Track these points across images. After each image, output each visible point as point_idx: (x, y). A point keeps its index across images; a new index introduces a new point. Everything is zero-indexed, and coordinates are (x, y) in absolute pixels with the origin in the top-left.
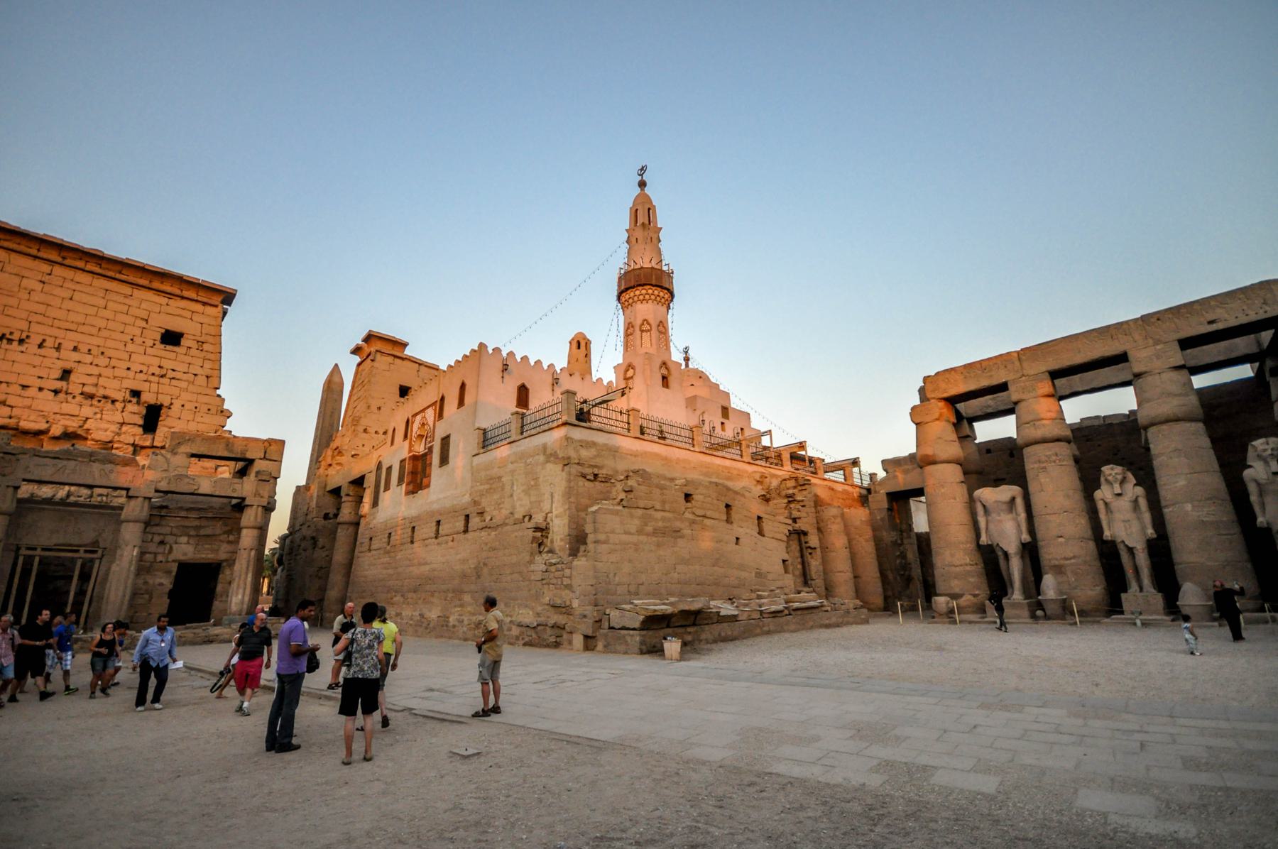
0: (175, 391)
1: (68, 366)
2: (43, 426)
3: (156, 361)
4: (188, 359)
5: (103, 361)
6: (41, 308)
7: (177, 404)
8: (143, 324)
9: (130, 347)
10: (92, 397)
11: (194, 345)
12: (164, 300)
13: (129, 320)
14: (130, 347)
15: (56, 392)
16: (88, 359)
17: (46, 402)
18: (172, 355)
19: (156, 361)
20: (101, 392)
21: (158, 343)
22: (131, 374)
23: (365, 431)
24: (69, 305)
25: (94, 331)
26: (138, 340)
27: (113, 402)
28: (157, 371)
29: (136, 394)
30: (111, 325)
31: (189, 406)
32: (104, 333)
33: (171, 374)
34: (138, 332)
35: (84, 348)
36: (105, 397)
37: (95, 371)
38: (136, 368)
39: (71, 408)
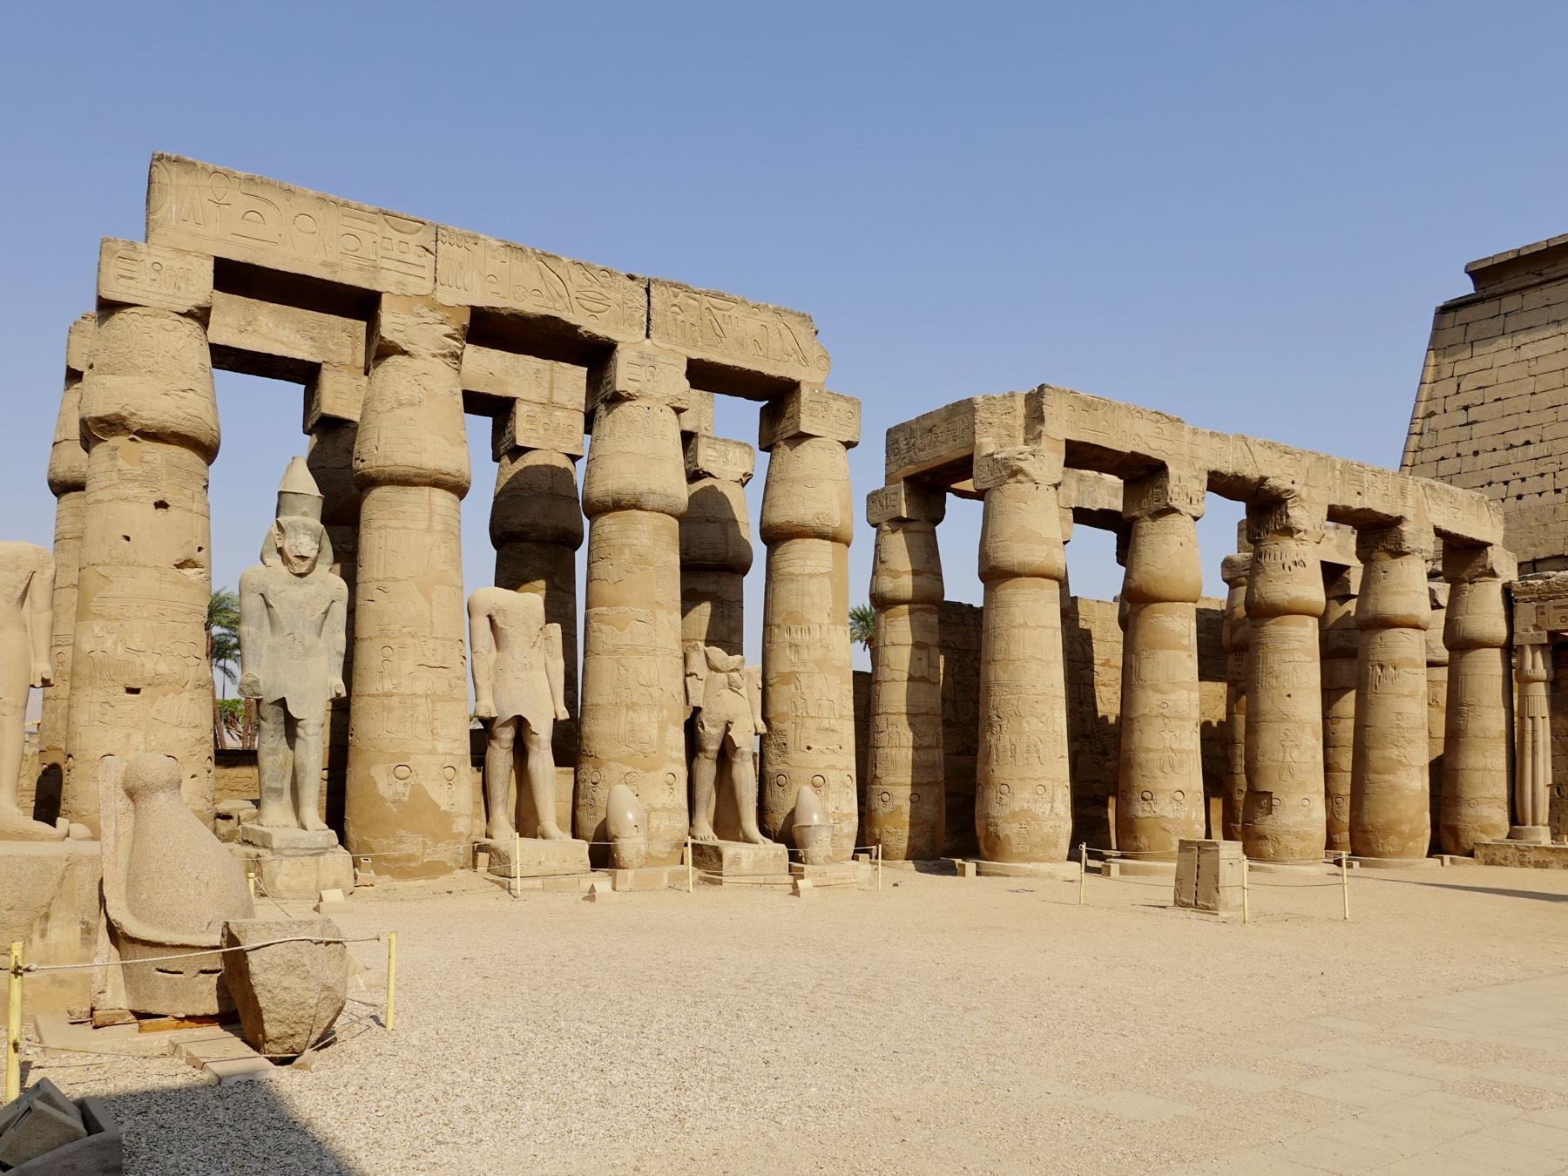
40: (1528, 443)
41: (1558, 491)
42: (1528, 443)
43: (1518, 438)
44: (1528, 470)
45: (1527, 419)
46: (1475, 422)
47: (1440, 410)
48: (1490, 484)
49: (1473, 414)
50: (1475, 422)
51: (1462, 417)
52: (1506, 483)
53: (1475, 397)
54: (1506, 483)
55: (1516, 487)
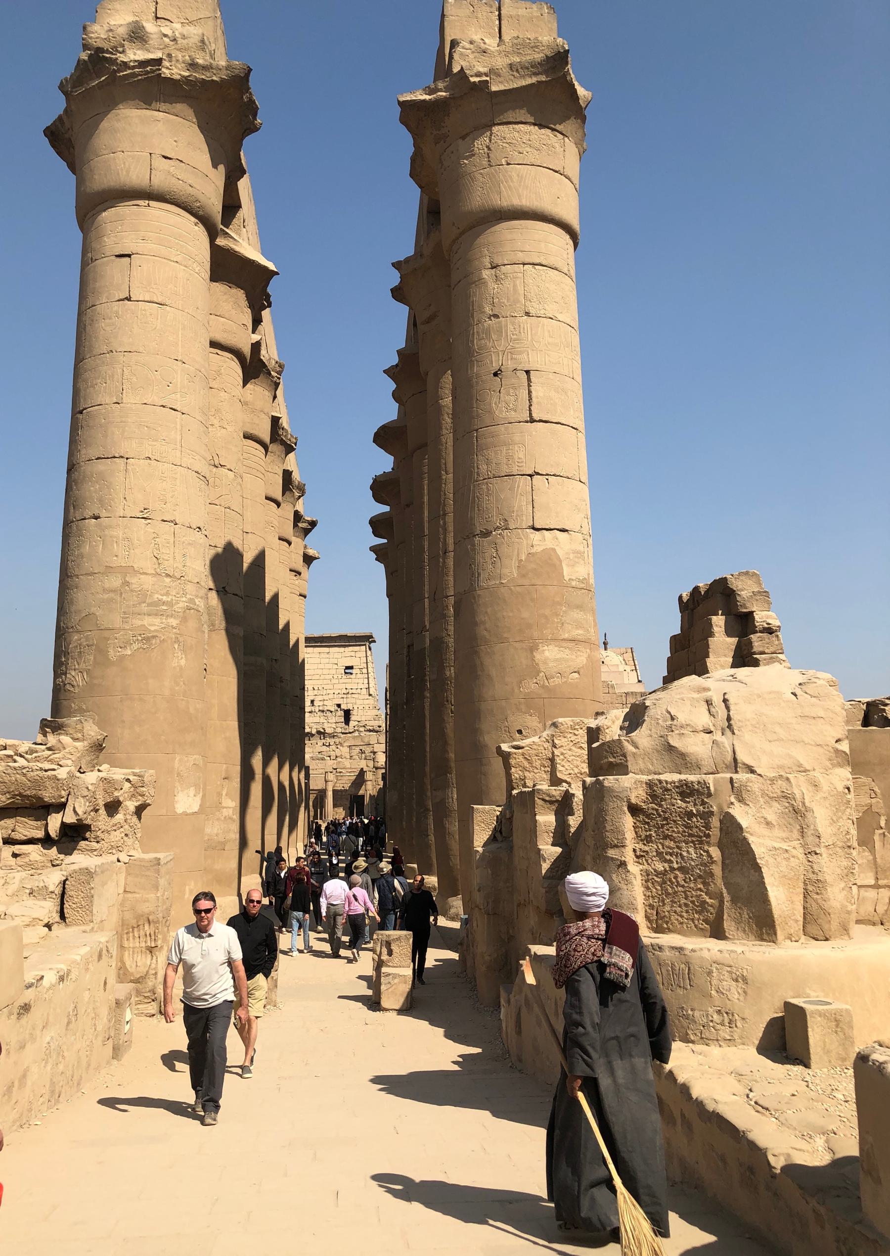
0: (353, 701)
3: (344, 686)
4: (357, 681)
7: (356, 708)
8: (336, 666)
9: (334, 681)
10: (323, 711)
11: (358, 671)
12: (342, 649)
13: (330, 666)
14: (334, 681)
19: (344, 686)
20: (326, 708)
25: (318, 677)
26: (335, 677)
29: (339, 706)
30: (325, 672)
31: (361, 707)
33: (351, 691)
34: (334, 672)
37: (321, 698)
39: (317, 719)
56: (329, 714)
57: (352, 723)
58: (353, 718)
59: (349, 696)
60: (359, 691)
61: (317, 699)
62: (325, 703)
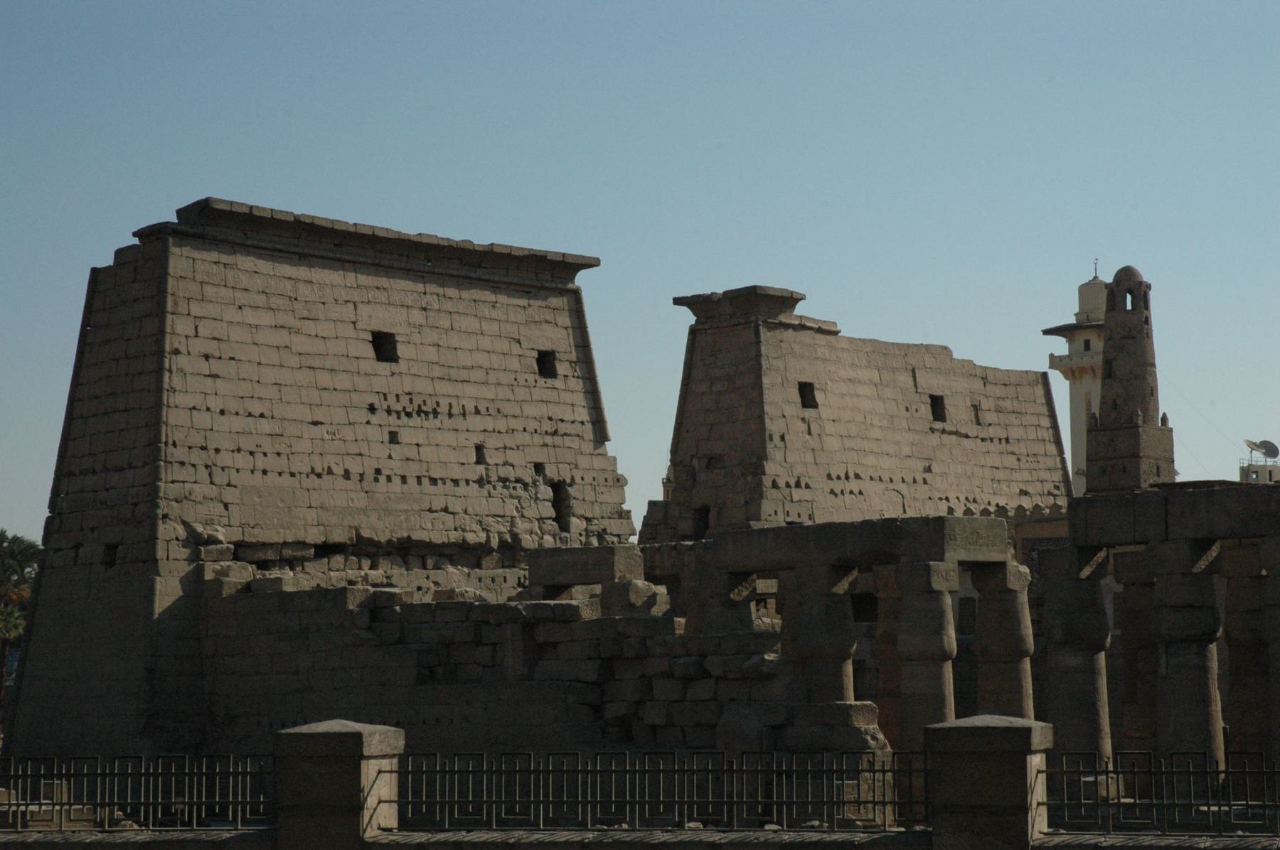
1: (477, 439)
2: (482, 537)
4: (567, 397)
5: (501, 424)
6: (432, 354)
8: (516, 349)
9: (521, 393)
13: (503, 345)
15: (480, 482)
16: (489, 423)
17: (478, 500)
18: (553, 395)
19: (542, 410)
21: (537, 377)
22: (526, 438)
23: (775, 485)
24: (454, 340)
27: (526, 485)
28: (548, 426)
30: (496, 361)
31: (588, 479)
32: (493, 377)
33: (563, 428)
34: (515, 364)
35: (483, 410)
36: (518, 481)
38: (533, 425)
40: (262, 416)
41: (292, 475)
42: (262, 416)
43: (257, 408)
44: (267, 446)
45: (259, 391)
46: (216, 376)
47: (183, 349)
48: (239, 450)
49: (215, 366)
50: (216, 376)
51: (204, 367)
52: (252, 453)
53: (212, 348)
54: (252, 453)
55: (261, 462)
56: (520, 491)
57: (576, 524)
58: (578, 507)
59: (558, 440)
60: (577, 428)
61: (491, 442)
62: (512, 456)
